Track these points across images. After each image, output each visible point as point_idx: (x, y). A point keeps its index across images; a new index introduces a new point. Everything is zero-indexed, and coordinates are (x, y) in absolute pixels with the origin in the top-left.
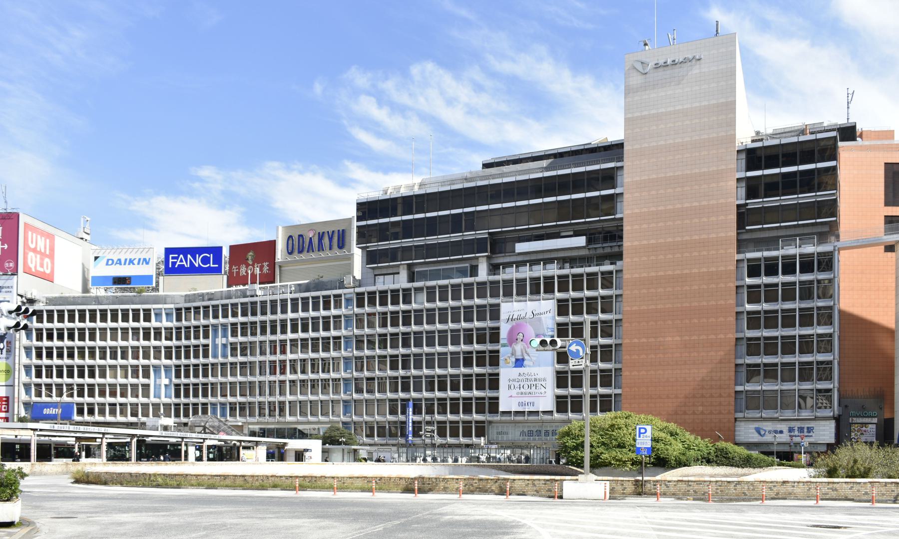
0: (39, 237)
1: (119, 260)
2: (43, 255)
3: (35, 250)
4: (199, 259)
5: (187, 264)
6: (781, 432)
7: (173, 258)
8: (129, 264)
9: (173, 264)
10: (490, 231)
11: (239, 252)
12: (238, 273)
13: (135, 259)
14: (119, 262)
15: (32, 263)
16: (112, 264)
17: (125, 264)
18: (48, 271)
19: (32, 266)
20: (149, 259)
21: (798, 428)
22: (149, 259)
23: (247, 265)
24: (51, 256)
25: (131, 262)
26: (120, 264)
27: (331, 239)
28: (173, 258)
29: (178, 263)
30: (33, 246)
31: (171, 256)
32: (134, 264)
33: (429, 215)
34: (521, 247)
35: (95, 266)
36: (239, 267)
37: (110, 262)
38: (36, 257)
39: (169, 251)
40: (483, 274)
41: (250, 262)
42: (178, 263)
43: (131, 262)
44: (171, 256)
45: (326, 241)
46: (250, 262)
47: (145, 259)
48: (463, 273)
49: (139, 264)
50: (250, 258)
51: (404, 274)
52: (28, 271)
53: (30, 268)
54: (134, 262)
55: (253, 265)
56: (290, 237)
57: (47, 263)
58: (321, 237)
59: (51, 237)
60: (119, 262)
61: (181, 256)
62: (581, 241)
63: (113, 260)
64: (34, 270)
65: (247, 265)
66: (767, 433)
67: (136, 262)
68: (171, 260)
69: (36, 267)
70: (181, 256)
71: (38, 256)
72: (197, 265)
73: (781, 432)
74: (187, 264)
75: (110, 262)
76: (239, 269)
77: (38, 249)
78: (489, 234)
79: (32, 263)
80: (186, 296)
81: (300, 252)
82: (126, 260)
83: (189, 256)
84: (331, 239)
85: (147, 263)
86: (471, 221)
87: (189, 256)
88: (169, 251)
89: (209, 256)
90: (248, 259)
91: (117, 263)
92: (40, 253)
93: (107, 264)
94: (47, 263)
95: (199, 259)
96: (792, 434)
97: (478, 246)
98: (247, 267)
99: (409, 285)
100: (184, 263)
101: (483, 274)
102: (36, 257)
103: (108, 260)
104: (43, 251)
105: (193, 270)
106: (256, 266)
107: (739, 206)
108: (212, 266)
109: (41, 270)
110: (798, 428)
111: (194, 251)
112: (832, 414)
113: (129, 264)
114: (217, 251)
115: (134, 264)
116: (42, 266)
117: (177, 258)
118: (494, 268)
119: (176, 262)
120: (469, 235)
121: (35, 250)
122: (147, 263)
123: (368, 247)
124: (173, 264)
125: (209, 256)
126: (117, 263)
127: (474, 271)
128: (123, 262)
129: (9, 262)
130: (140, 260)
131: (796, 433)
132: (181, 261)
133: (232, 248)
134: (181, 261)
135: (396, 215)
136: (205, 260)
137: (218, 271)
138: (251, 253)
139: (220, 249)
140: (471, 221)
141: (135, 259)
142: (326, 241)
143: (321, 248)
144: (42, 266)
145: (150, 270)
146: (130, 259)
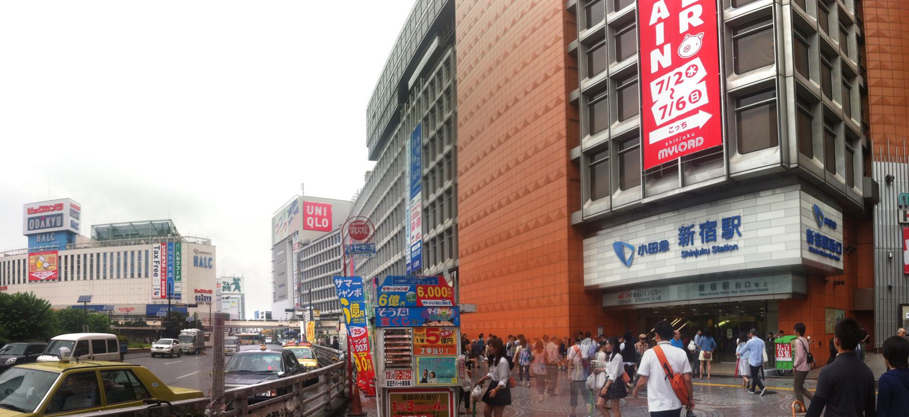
0: (317, 208)
3: (313, 216)
15: (310, 222)
19: (311, 225)
30: (312, 213)
53: (310, 227)
69: (314, 225)
71: (316, 219)
77: (316, 214)
92: (318, 216)
104: (320, 214)
109: (320, 226)
116: (320, 222)
121: (313, 216)
144: (320, 222)
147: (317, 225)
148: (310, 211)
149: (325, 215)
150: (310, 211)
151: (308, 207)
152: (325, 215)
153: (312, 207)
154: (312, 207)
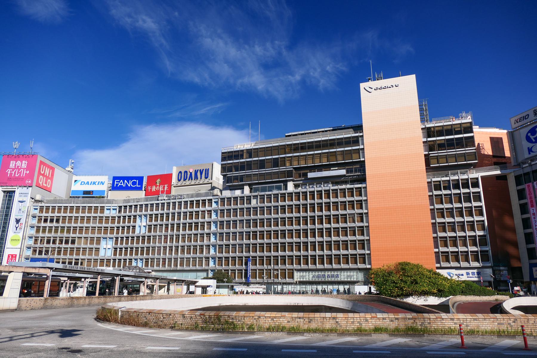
1: (88, 182)
2: (47, 178)
3: (43, 175)
4: (131, 182)
5: (124, 185)
6: (462, 275)
7: (117, 182)
8: (93, 184)
9: (117, 185)
10: (294, 167)
11: (152, 180)
12: (151, 190)
13: (96, 182)
15: (41, 181)
16: (84, 184)
17: (91, 184)
18: (49, 186)
19: (41, 183)
20: (104, 182)
21: (472, 273)
22: (104, 182)
23: (156, 186)
24: (52, 179)
25: (94, 183)
26: (88, 184)
27: (201, 173)
28: (117, 182)
29: (119, 184)
30: (42, 173)
31: (116, 181)
32: (95, 184)
33: (260, 158)
34: (311, 175)
35: (74, 185)
36: (152, 187)
37: (83, 183)
38: (43, 178)
39: (115, 178)
41: (158, 184)
42: (119, 184)
43: (94, 183)
44: (116, 181)
45: (199, 174)
46: (158, 184)
47: (102, 182)
48: (279, 188)
49: (98, 184)
50: (158, 182)
51: (247, 189)
52: (38, 186)
53: (40, 184)
54: (96, 183)
55: (159, 186)
56: (180, 172)
57: (49, 182)
58: (196, 172)
59: (53, 169)
60: (88, 183)
61: (122, 181)
62: (343, 172)
63: (84, 182)
64: (41, 185)
65: (156, 186)
66: (454, 275)
67: (97, 183)
68: (116, 183)
69: (42, 184)
70: (122, 181)
71: (45, 178)
72: (129, 186)
73: (462, 275)
74: (124, 185)
75: (83, 183)
76: (152, 188)
77: (45, 174)
78: (293, 168)
79: (41, 181)
80: (124, 200)
82: (92, 182)
83: (126, 181)
84: (201, 173)
85: (103, 184)
87: (126, 181)
88: (115, 178)
89: (136, 181)
90: (157, 183)
91: (86, 184)
93: (81, 184)
94: (49, 182)
95: (131, 182)
96: (469, 276)
98: (156, 187)
99: (250, 194)
100: (123, 184)
102: (43, 178)
103: (82, 182)
105: (127, 188)
106: (161, 186)
107: (425, 155)
108: (137, 186)
109: (45, 185)
110: (472, 273)
111: (128, 179)
112: (490, 264)
113: (93, 184)
114: (141, 179)
115: (95, 184)
117: (119, 182)
118: (296, 186)
119: (118, 184)
122: (103, 184)
123: (227, 175)
124: (117, 185)
125: (136, 181)
126: (86, 184)
127: (286, 189)
128: (90, 183)
129: (28, 180)
130: (99, 182)
131: (471, 275)
132: (121, 183)
133: (149, 177)
134: (121, 183)
135: (243, 159)
136: (134, 183)
137: (140, 189)
138: (159, 180)
139: (143, 177)
141: (96, 182)
142: (199, 174)
144: (46, 183)
145: (105, 188)
146: (94, 182)
147: (44, 185)
148: (42, 171)
149: (50, 177)
150: (42, 171)
151: (42, 166)
152: (50, 177)
153: (44, 167)
154: (44, 167)
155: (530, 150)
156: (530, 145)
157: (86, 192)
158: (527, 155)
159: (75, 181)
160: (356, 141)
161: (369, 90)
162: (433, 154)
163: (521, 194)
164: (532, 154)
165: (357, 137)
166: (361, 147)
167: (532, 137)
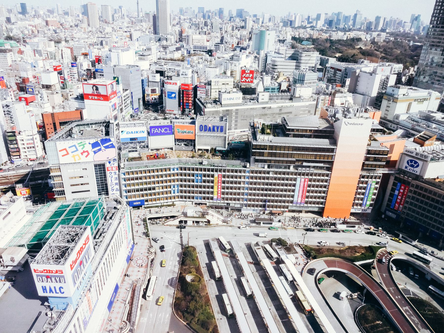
14: (132, 132)
25: (137, 132)
40: (292, 169)
43: (137, 132)
48: (285, 168)
60: (132, 132)
67: (139, 132)
81: (205, 131)
84: (218, 128)
86: (291, 155)
97: (291, 162)
101: (292, 169)
120: (290, 159)
127: (289, 168)
140: (291, 155)
142: (216, 128)
143: (214, 130)
155: (406, 167)
156: (407, 166)
157: (132, 139)
158: (404, 168)
159: (122, 132)
160: (332, 150)
161: (347, 124)
162: (367, 163)
163: (394, 184)
164: (406, 169)
165: (334, 149)
166: (334, 154)
167: (410, 163)
